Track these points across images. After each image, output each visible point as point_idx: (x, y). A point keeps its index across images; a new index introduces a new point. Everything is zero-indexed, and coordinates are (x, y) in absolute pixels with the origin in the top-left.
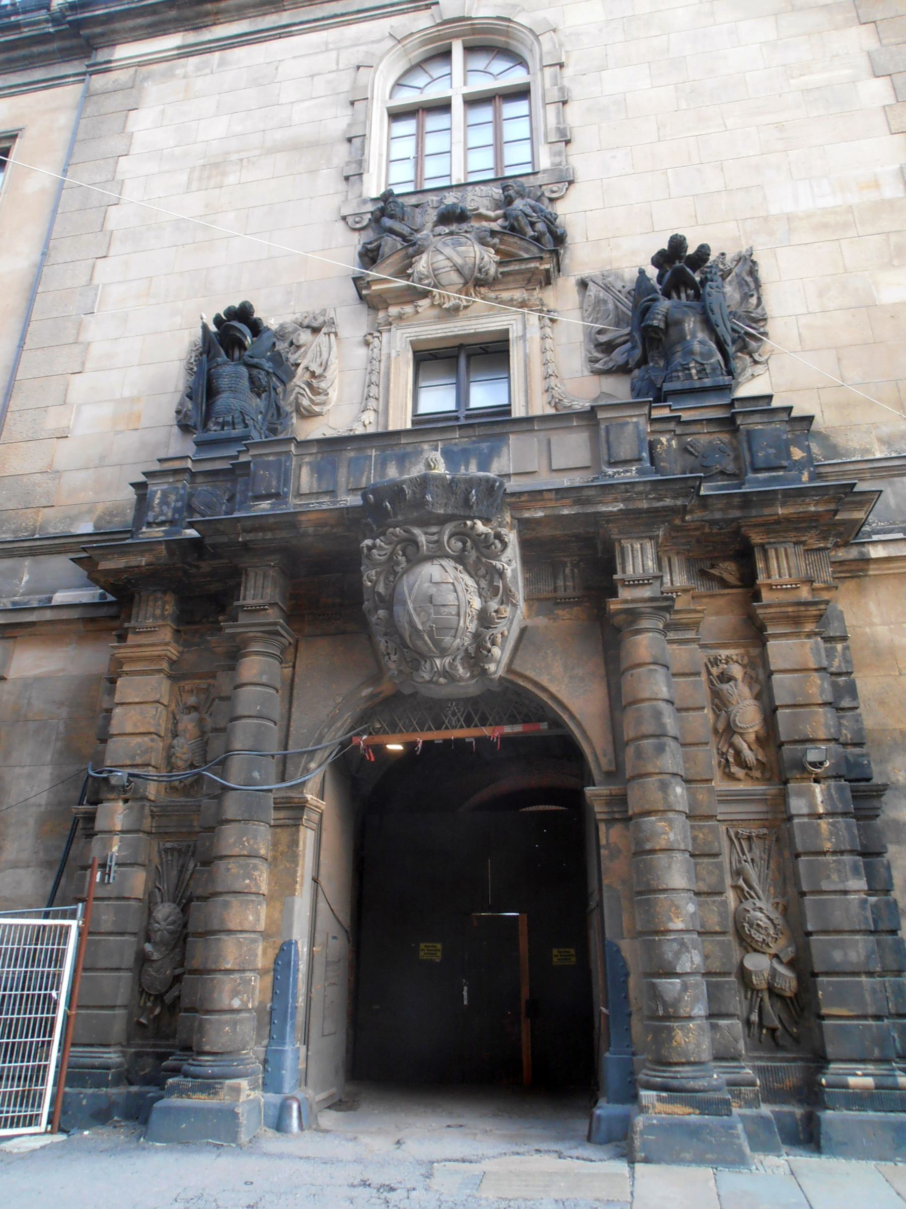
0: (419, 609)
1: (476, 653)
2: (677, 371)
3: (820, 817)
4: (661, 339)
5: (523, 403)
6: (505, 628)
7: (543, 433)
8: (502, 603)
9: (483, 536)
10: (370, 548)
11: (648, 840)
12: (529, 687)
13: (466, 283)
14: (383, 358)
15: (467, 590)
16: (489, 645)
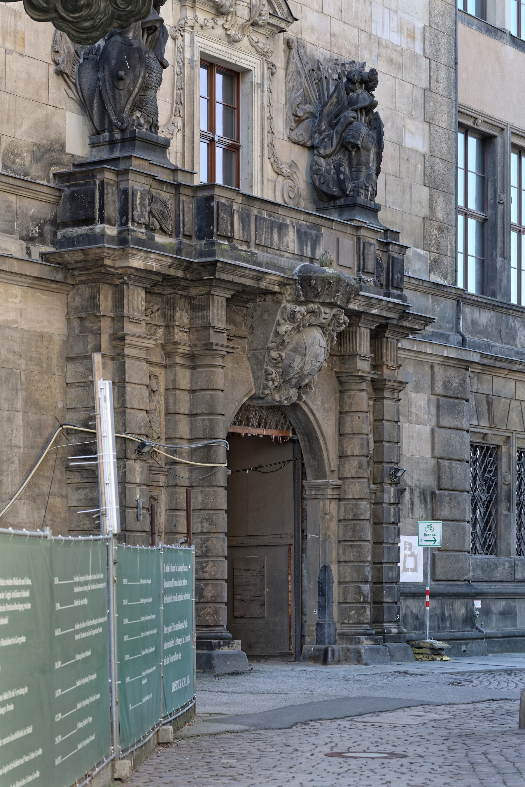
2: (362, 188)
3: (390, 504)
4: (350, 152)
5: (259, 154)
11: (362, 514)
13: (248, 21)
14: (186, 62)
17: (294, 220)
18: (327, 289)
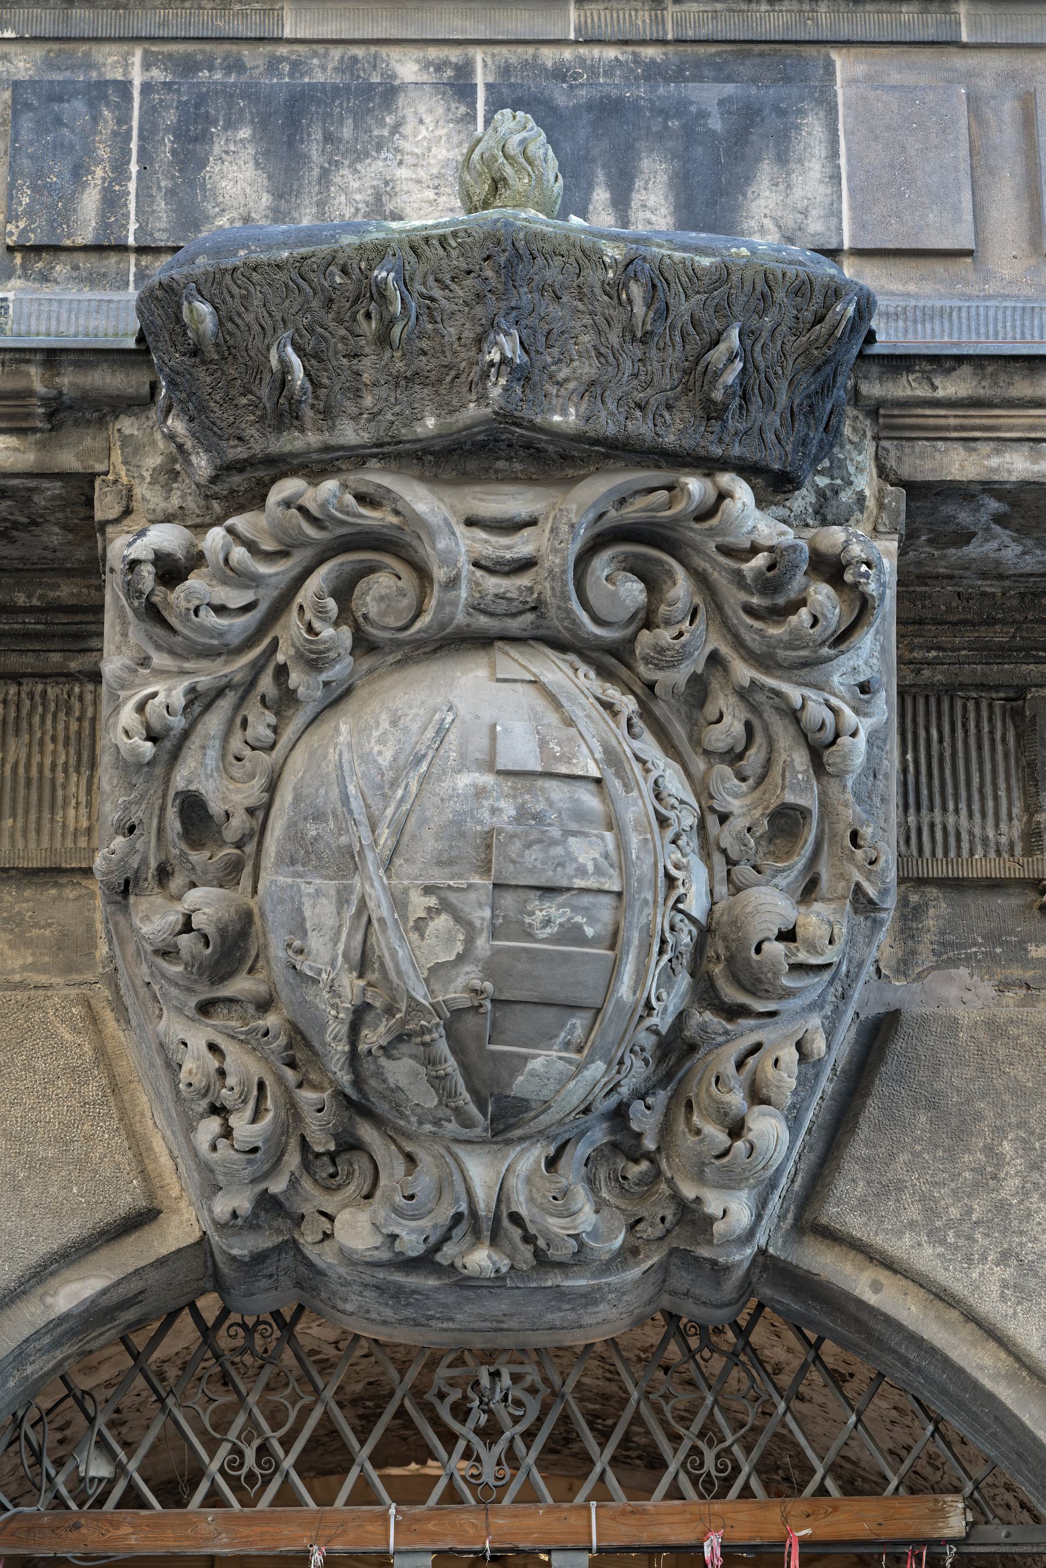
0: (419, 903)
1: (666, 1129)
6: (815, 1021)
7: (995, 63)
8: (809, 890)
9: (760, 561)
10: (171, 571)
12: (907, 1309)
15: (663, 822)
16: (737, 1099)
17: (478, 55)
18: (383, 339)
